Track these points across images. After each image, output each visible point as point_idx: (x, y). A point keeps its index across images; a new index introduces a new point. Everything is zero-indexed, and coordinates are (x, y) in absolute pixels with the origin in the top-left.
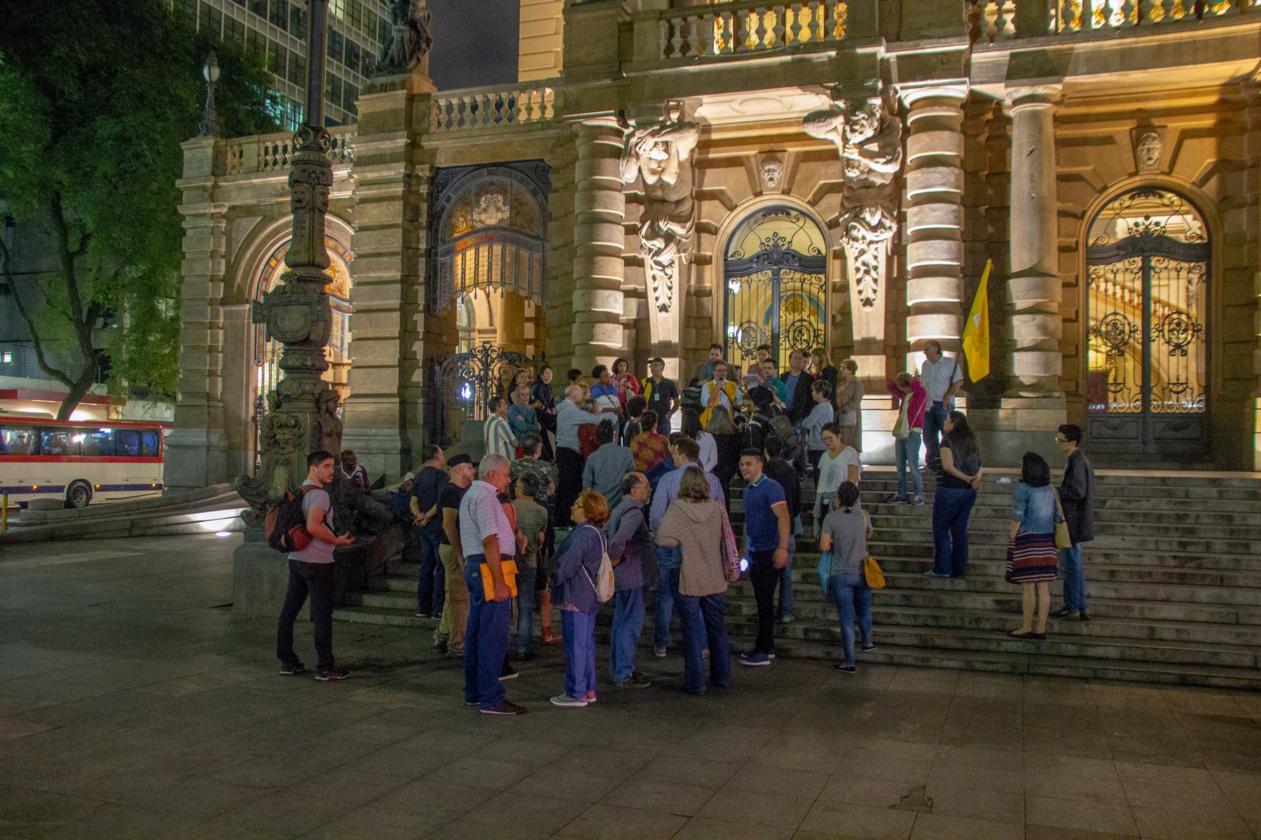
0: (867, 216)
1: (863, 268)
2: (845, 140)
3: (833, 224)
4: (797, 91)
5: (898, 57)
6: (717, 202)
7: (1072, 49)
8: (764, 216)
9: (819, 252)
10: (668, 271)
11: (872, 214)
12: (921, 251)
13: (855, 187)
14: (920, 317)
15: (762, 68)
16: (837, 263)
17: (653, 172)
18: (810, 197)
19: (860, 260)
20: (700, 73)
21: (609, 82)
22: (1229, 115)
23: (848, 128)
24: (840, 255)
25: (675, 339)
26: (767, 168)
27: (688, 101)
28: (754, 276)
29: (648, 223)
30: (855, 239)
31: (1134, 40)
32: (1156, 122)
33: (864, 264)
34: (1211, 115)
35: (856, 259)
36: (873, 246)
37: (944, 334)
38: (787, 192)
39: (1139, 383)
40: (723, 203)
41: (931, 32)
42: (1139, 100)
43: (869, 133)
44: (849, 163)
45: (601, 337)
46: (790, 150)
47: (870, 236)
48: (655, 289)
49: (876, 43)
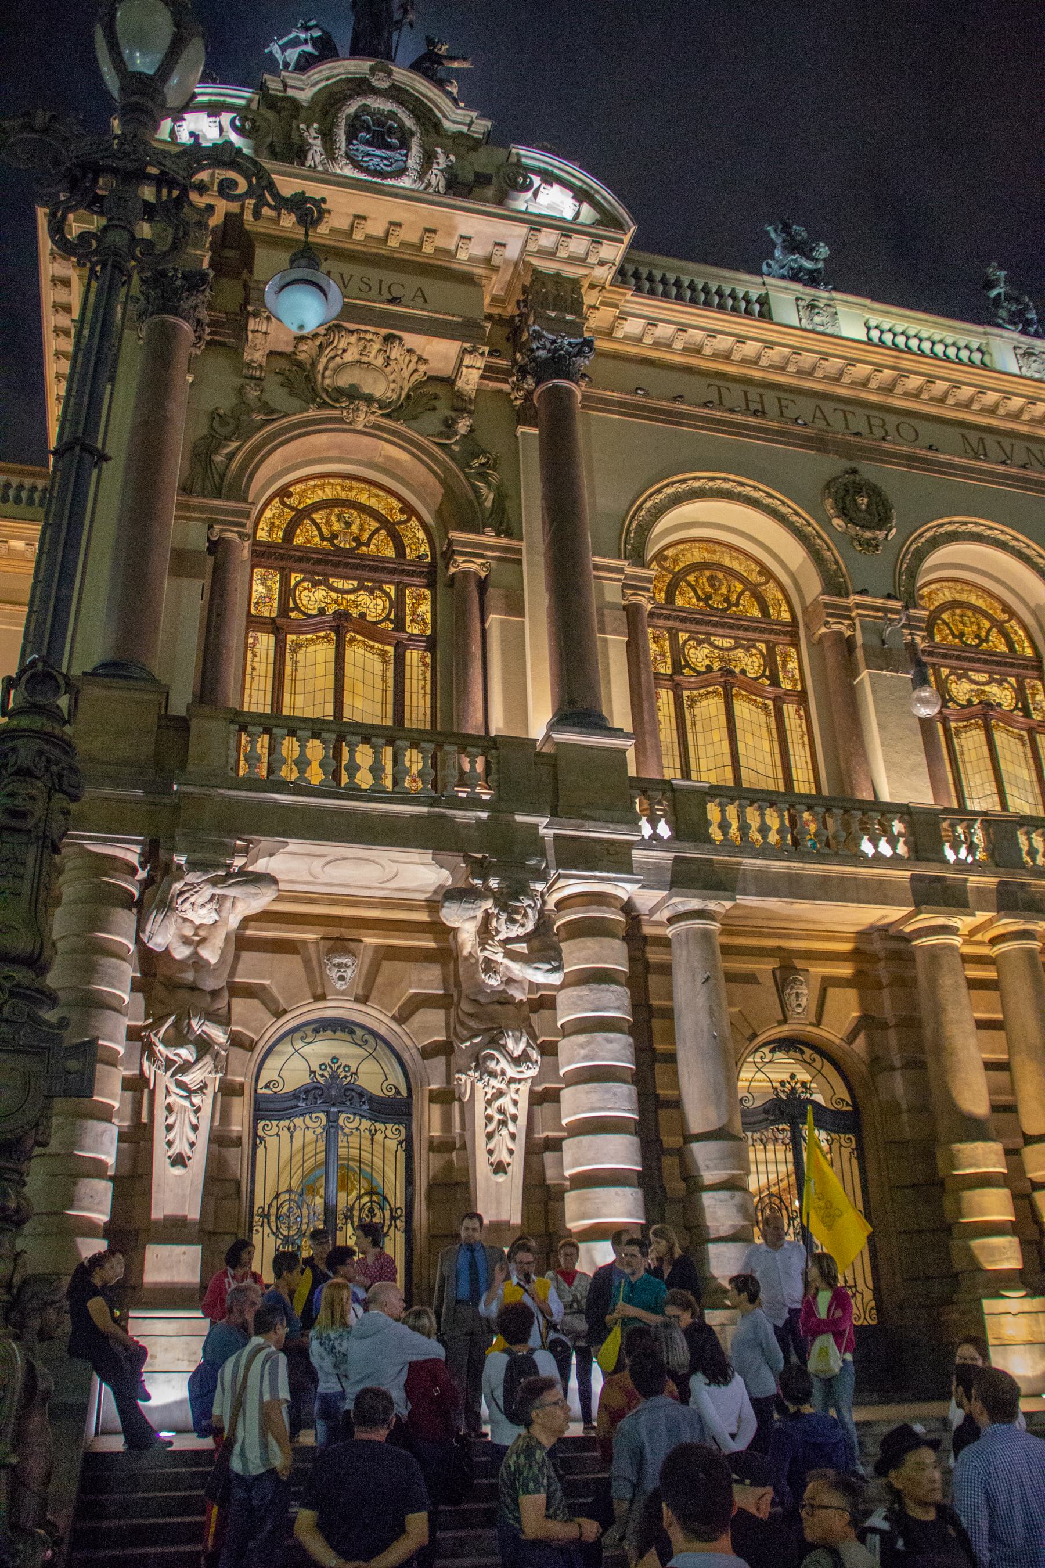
0: (510, 1044)
1: (498, 1117)
2: (485, 932)
3: (445, 1049)
4: (428, 856)
5: (556, 836)
6: (256, 1002)
7: (740, 864)
8: (316, 1031)
9: (398, 1092)
10: (196, 1100)
11: (517, 1041)
12: (594, 1097)
13: (481, 999)
14: (598, 1189)
15: (384, 816)
16: (436, 1110)
17: (186, 941)
18: (395, 1011)
19: (500, 1102)
20: (293, 808)
21: (140, 793)
22: (865, 966)
23: (504, 916)
24: (446, 1097)
25: (193, 1213)
26: (336, 961)
27: (266, 842)
28: (298, 1121)
29: (172, 1019)
30: (493, 1074)
31: (801, 865)
32: (799, 964)
33: (500, 1111)
34: (850, 964)
35: (489, 1103)
36: (513, 1086)
37: (631, 1216)
38: (363, 999)
39: (870, 1284)
40: (264, 1003)
41: (597, 814)
42: (781, 936)
43: (530, 926)
44: (490, 966)
45: (86, 1202)
46: (366, 940)
47: (511, 1072)
48: (169, 1128)
49: (537, 812)
